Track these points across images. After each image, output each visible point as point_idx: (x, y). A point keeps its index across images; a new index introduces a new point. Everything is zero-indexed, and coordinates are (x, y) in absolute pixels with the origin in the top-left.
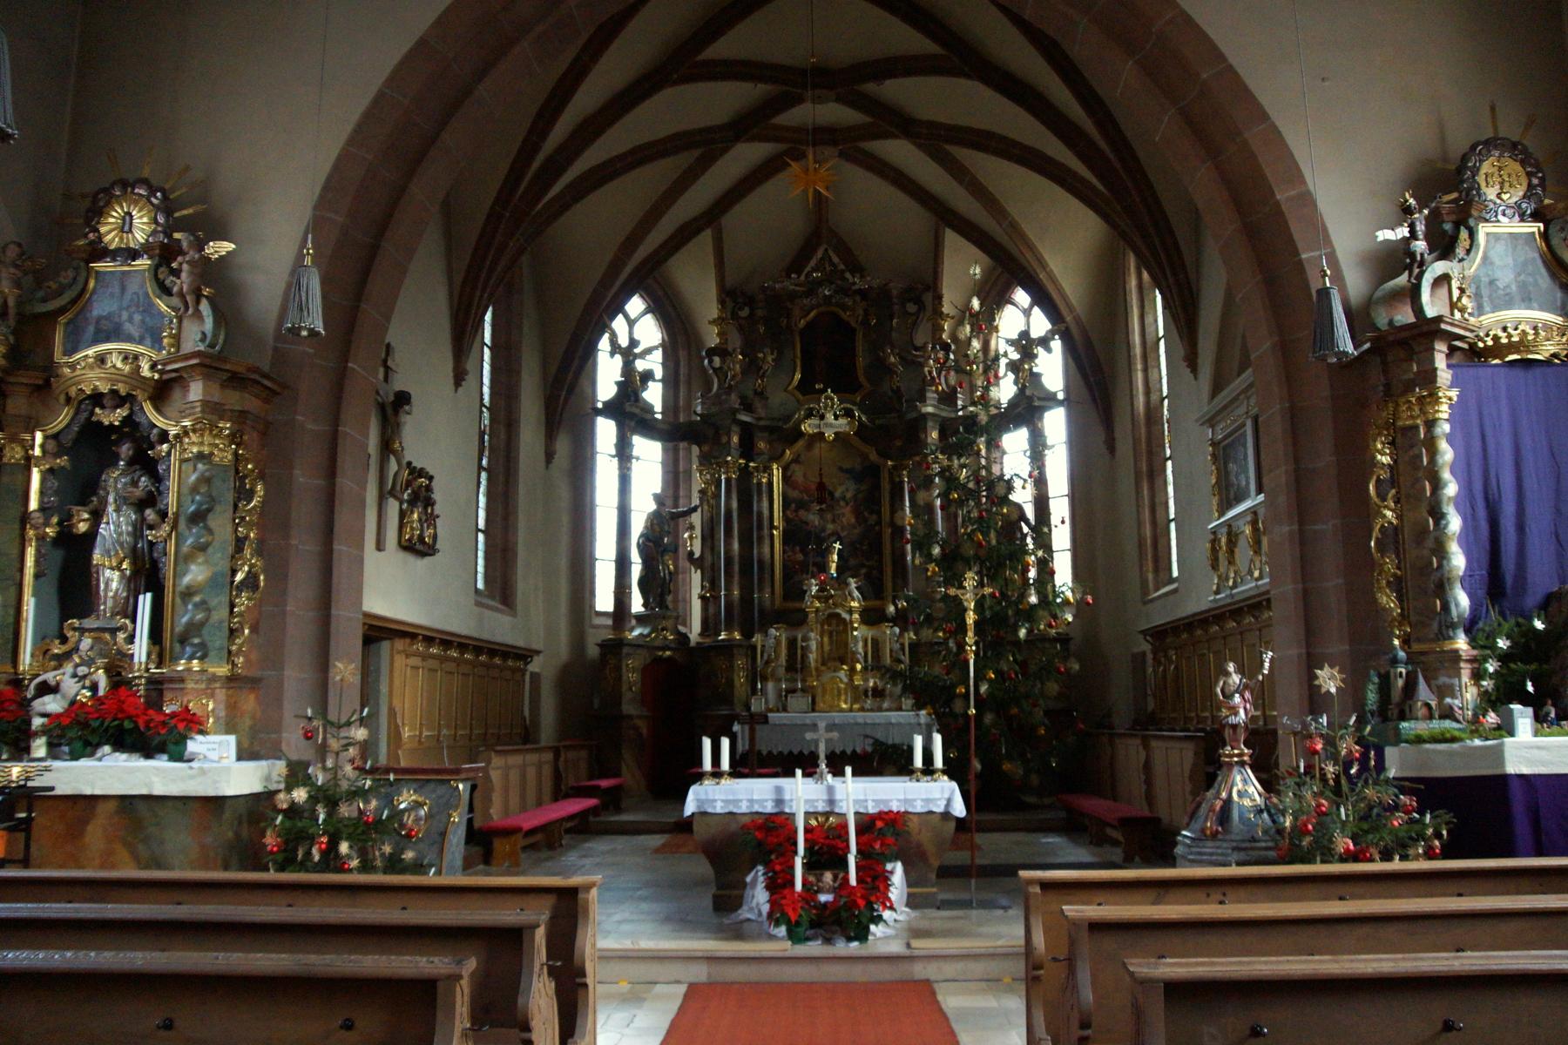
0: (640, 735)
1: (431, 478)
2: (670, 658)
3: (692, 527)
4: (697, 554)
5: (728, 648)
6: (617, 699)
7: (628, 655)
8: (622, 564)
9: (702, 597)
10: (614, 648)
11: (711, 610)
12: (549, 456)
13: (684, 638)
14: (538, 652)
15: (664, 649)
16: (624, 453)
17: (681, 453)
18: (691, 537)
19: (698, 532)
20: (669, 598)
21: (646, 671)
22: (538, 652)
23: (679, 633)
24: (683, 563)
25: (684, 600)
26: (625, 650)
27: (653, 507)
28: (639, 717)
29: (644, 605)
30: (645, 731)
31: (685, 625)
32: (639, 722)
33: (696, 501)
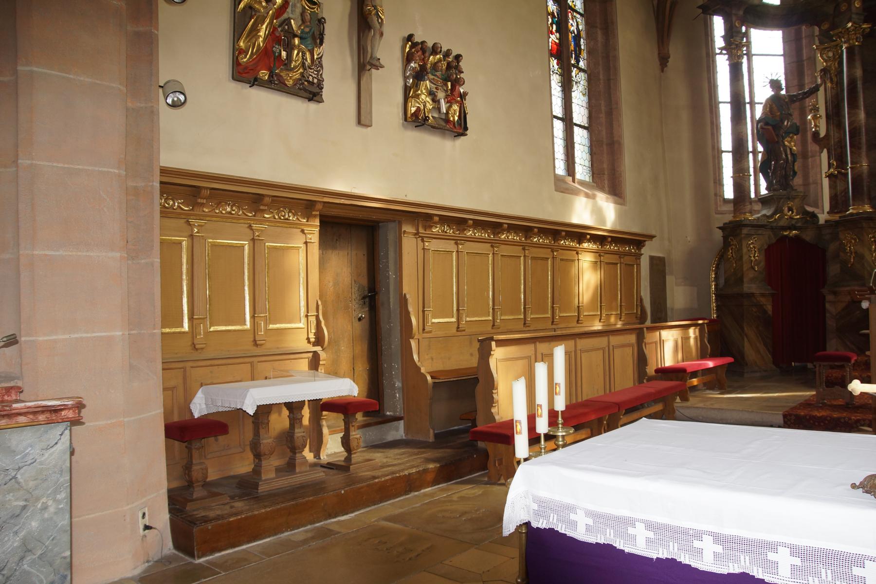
0: (765, 312)
1: (458, 57)
2: (796, 236)
3: (816, 109)
4: (823, 133)
5: (855, 223)
6: (740, 281)
7: (749, 236)
8: (739, 151)
9: (830, 176)
10: (732, 230)
11: (840, 188)
12: (664, 60)
13: (814, 216)
14: (651, 237)
15: (791, 228)
16: (736, 45)
17: (804, 41)
18: (815, 118)
19: (822, 112)
20: (797, 181)
21: (769, 252)
22: (651, 237)
23: (806, 213)
24: (812, 147)
25: (815, 183)
26: (745, 231)
27: (769, 93)
28: (763, 295)
29: (767, 189)
30: (769, 308)
31: (817, 207)
32: (763, 300)
33: (819, 81)
